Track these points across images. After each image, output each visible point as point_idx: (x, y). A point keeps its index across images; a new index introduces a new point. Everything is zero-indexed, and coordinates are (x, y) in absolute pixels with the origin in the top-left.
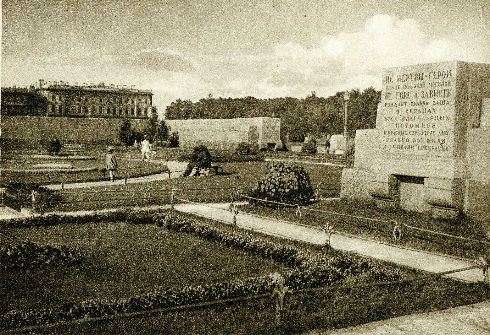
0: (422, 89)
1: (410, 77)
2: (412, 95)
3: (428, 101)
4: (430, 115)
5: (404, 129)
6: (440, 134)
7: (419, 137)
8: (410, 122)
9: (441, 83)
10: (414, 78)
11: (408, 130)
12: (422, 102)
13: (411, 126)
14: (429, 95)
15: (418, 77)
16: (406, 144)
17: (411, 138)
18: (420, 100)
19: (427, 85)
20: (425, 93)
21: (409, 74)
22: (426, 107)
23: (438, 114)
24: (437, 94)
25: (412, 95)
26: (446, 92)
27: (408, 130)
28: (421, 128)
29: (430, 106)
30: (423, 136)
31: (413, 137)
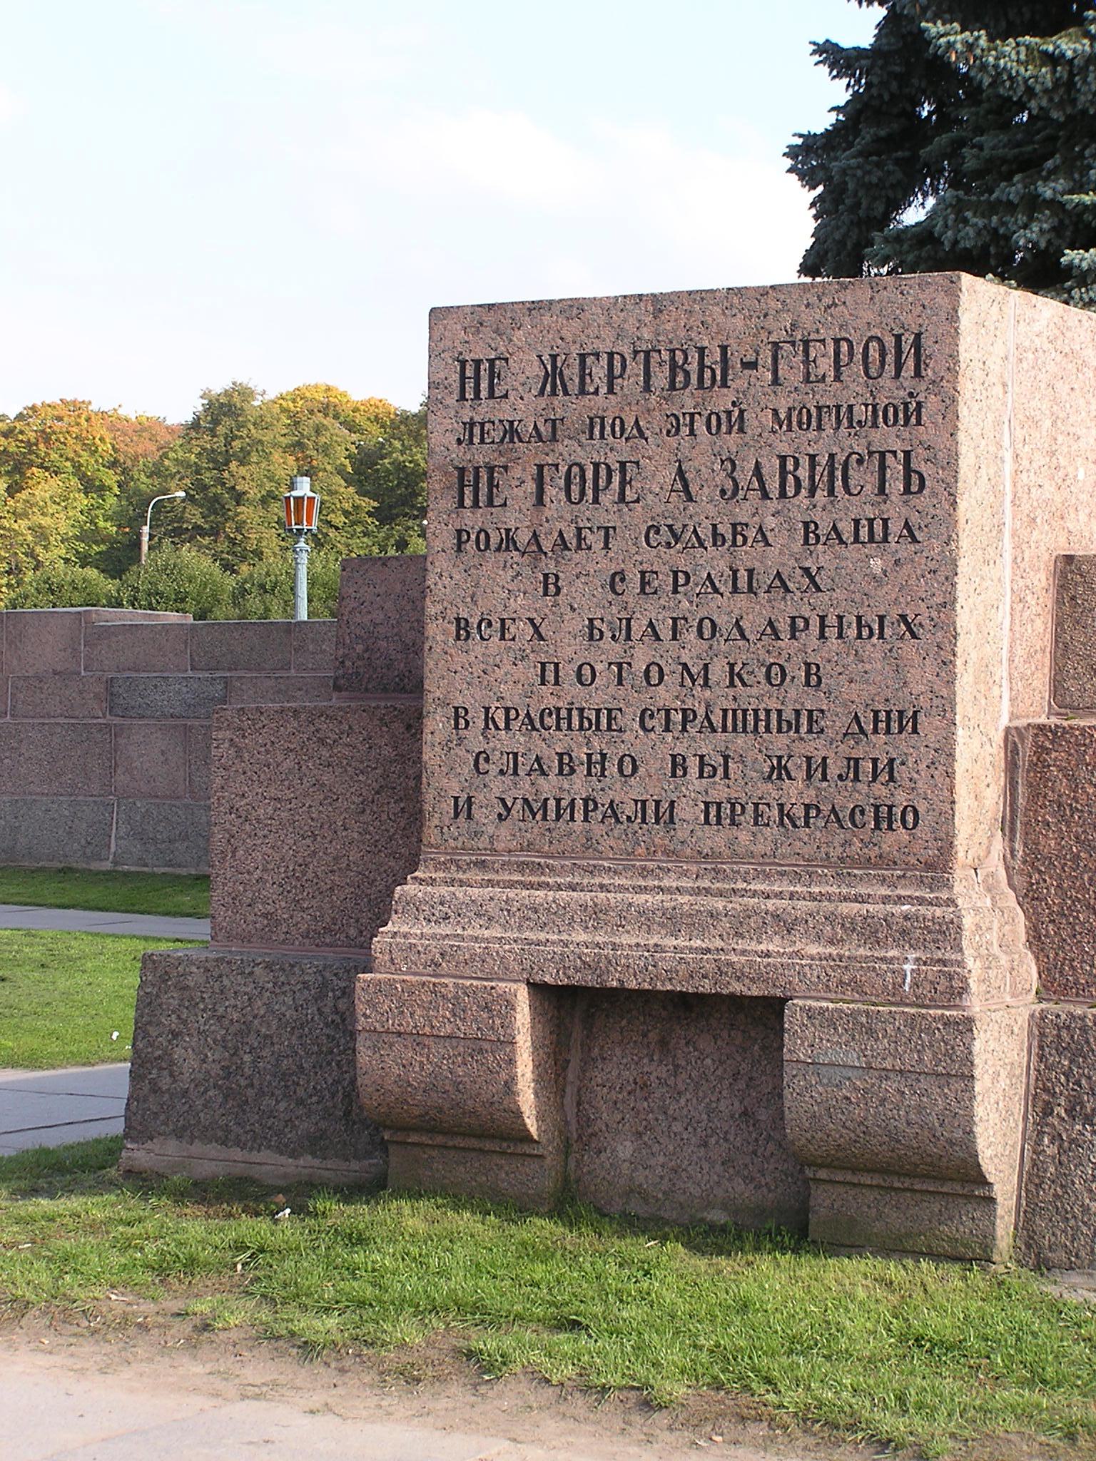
0: (732, 440)
1: (635, 368)
2: (657, 476)
3: (770, 522)
4: (783, 611)
5: (600, 695)
6: (856, 730)
7: (709, 746)
8: (641, 657)
9: (860, 413)
10: (660, 378)
11: (633, 701)
12: (724, 529)
13: (653, 676)
14: (773, 486)
15: (693, 367)
16: (625, 794)
17: (654, 750)
18: (707, 510)
19: (758, 420)
20: (745, 475)
21: (627, 351)
22: (747, 556)
23: (832, 602)
24: (835, 475)
25: (657, 476)
26: (896, 468)
27: (633, 701)
28: (721, 697)
29: (782, 553)
30: (741, 742)
31: (671, 743)
